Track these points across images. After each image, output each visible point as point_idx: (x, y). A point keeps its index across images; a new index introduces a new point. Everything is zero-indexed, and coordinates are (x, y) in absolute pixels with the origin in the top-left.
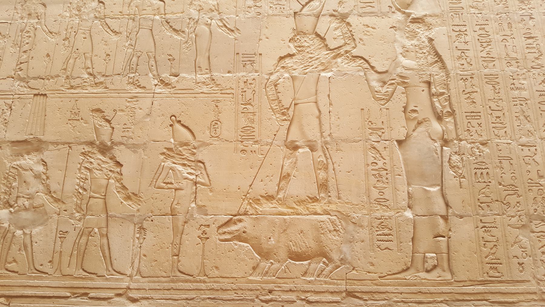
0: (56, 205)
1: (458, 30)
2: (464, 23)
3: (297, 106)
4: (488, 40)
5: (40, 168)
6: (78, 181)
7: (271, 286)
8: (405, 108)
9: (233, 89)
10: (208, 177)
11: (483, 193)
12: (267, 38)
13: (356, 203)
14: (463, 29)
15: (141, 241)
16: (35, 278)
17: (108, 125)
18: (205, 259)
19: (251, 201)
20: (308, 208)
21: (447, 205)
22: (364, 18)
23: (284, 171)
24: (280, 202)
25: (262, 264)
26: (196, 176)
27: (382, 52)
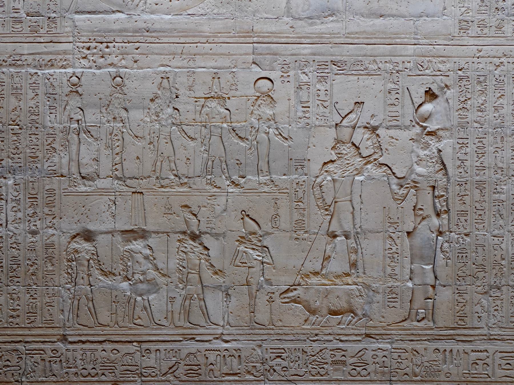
0: (164, 278)
1: (461, 142)
2: (467, 137)
3: (337, 204)
4: (484, 152)
5: (148, 252)
6: (178, 261)
7: (317, 332)
8: (415, 207)
10: (272, 258)
11: (462, 270)
12: (314, 146)
13: (375, 277)
14: (466, 141)
15: (228, 303)
16: (156, 329)
17: (195, 218)
20: (342, 281)
21: (436, 278)
22: (390, 131)
23: (326, 254)
25: (311, 318)
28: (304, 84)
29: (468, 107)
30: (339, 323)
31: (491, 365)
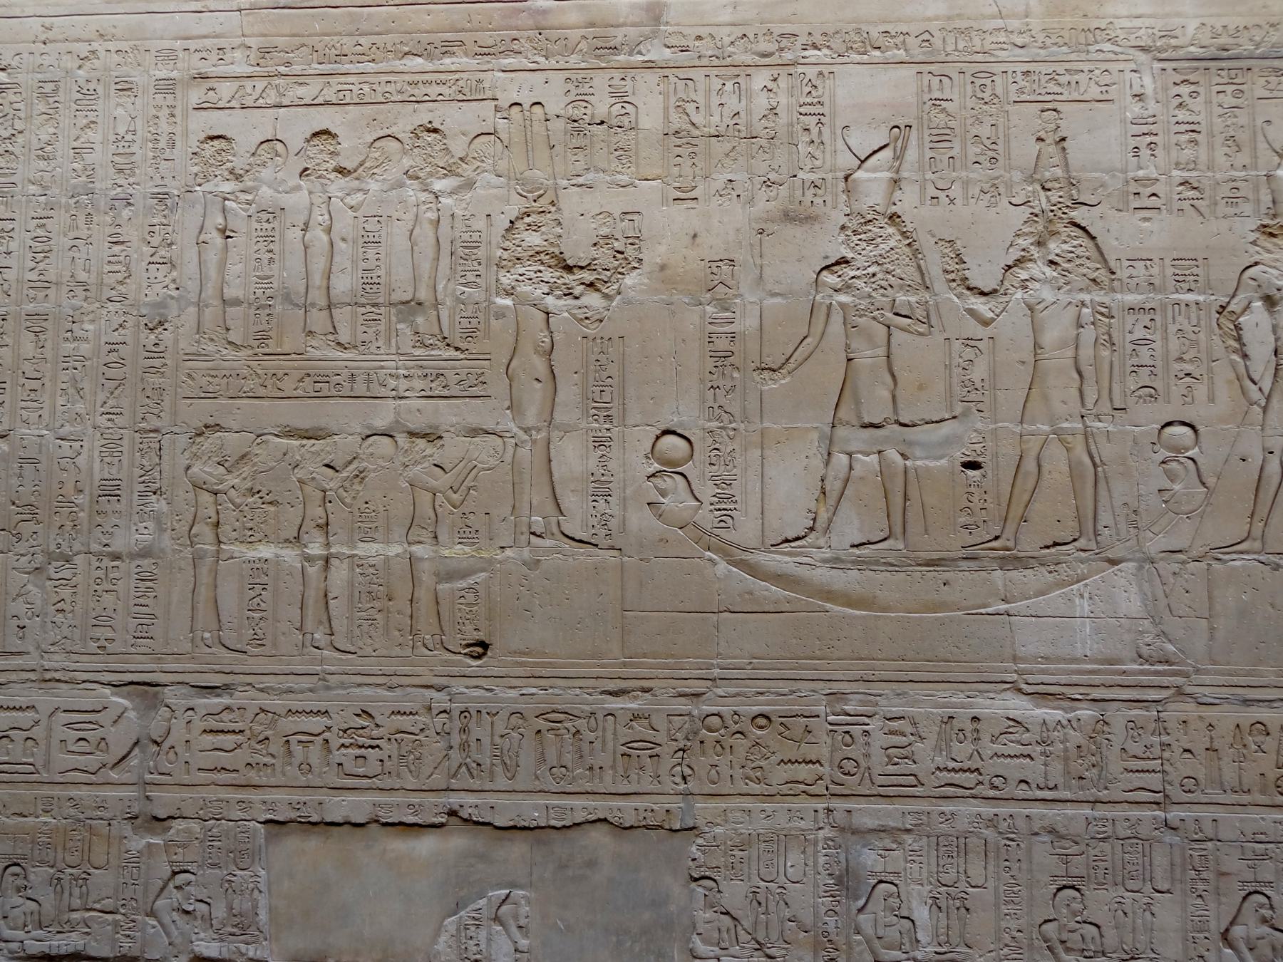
4: (47, 248)
29: (17, 150)
31: (42, 743)
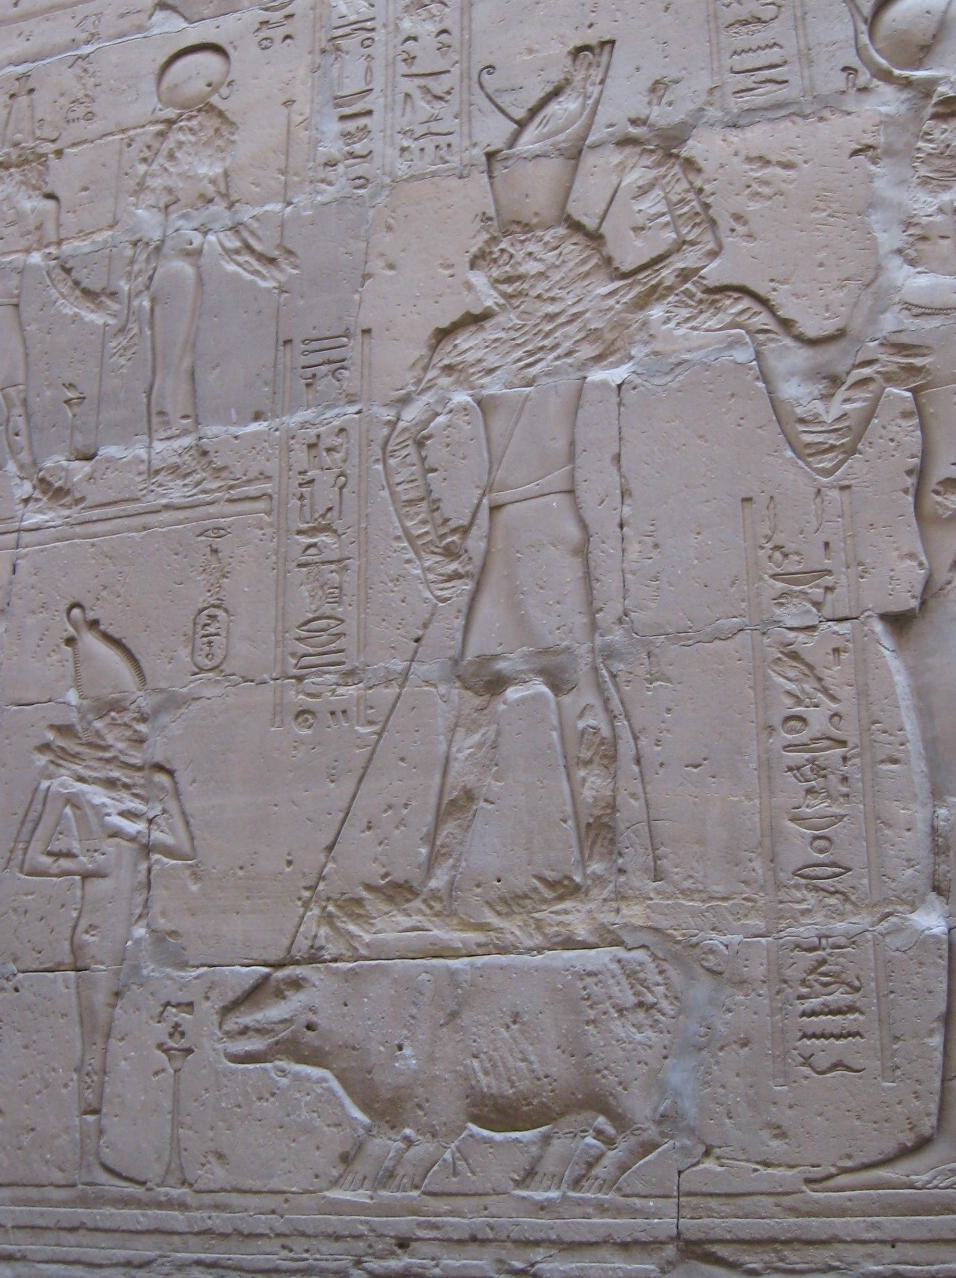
7: (404, 1224)
8: (921, 473)
9: (269, 478)
12: (391, 267)
13: (718, 889)
18: (181, 1125)
19: (331, 908)
20: (539, 925)
23: (450, 780)
24: (438, 906)
26: (150, 821)
27: (821, 256)
28: (347, 30)
30: (529, 1176)
